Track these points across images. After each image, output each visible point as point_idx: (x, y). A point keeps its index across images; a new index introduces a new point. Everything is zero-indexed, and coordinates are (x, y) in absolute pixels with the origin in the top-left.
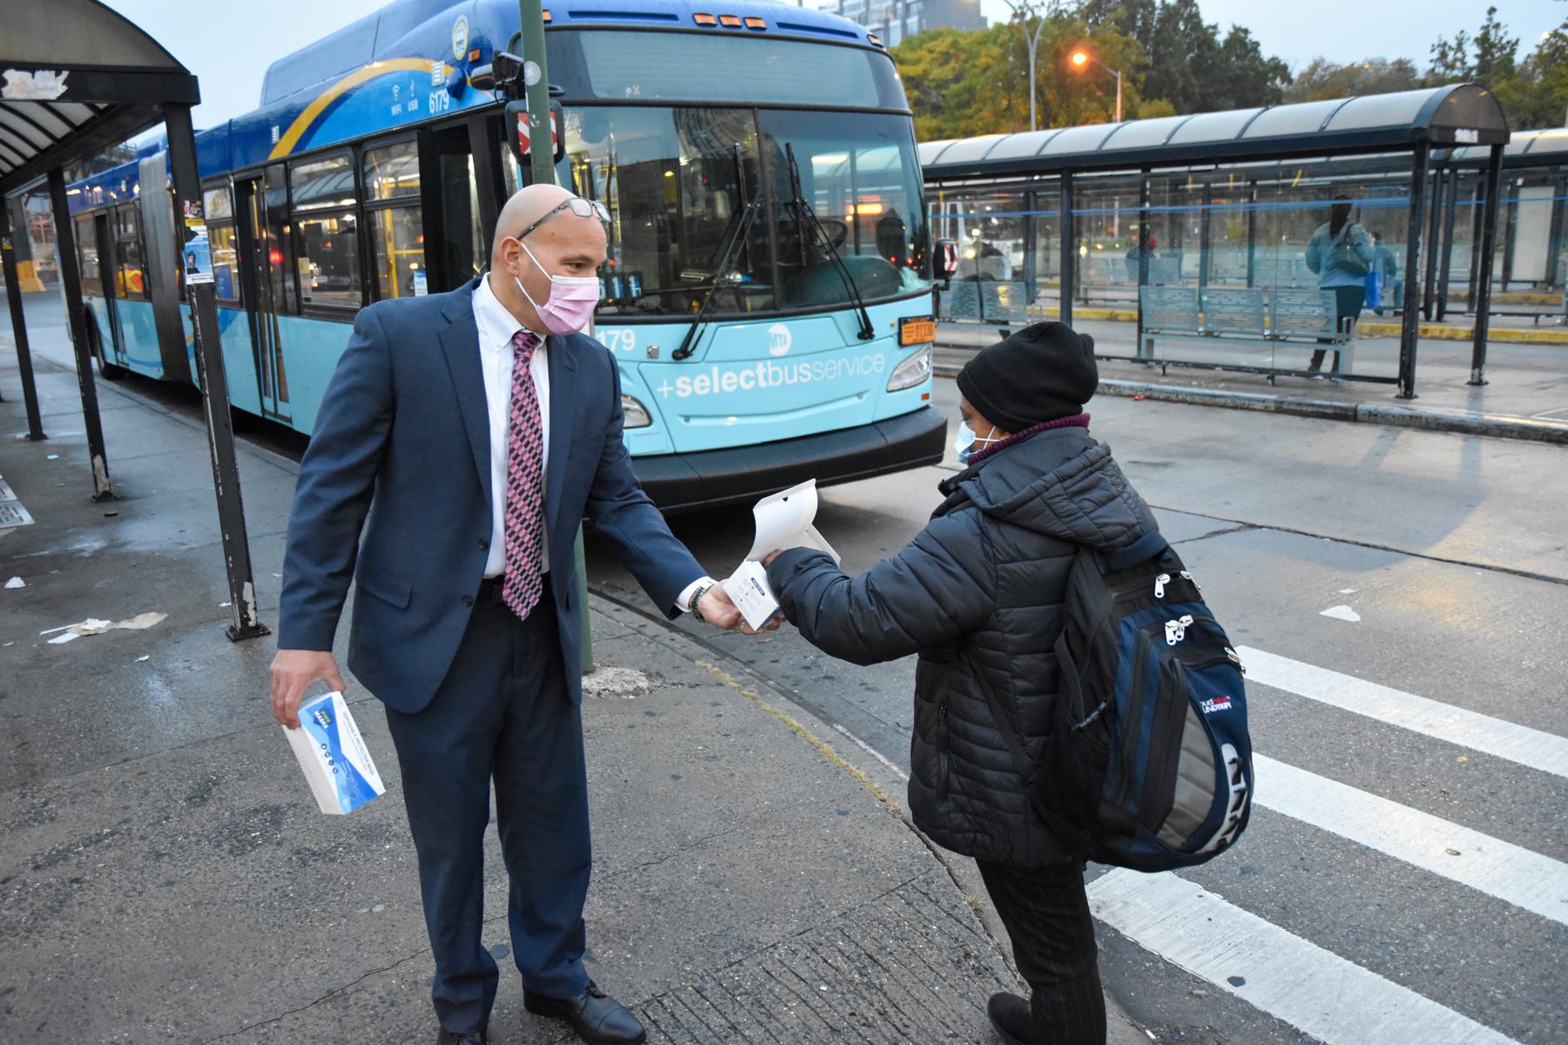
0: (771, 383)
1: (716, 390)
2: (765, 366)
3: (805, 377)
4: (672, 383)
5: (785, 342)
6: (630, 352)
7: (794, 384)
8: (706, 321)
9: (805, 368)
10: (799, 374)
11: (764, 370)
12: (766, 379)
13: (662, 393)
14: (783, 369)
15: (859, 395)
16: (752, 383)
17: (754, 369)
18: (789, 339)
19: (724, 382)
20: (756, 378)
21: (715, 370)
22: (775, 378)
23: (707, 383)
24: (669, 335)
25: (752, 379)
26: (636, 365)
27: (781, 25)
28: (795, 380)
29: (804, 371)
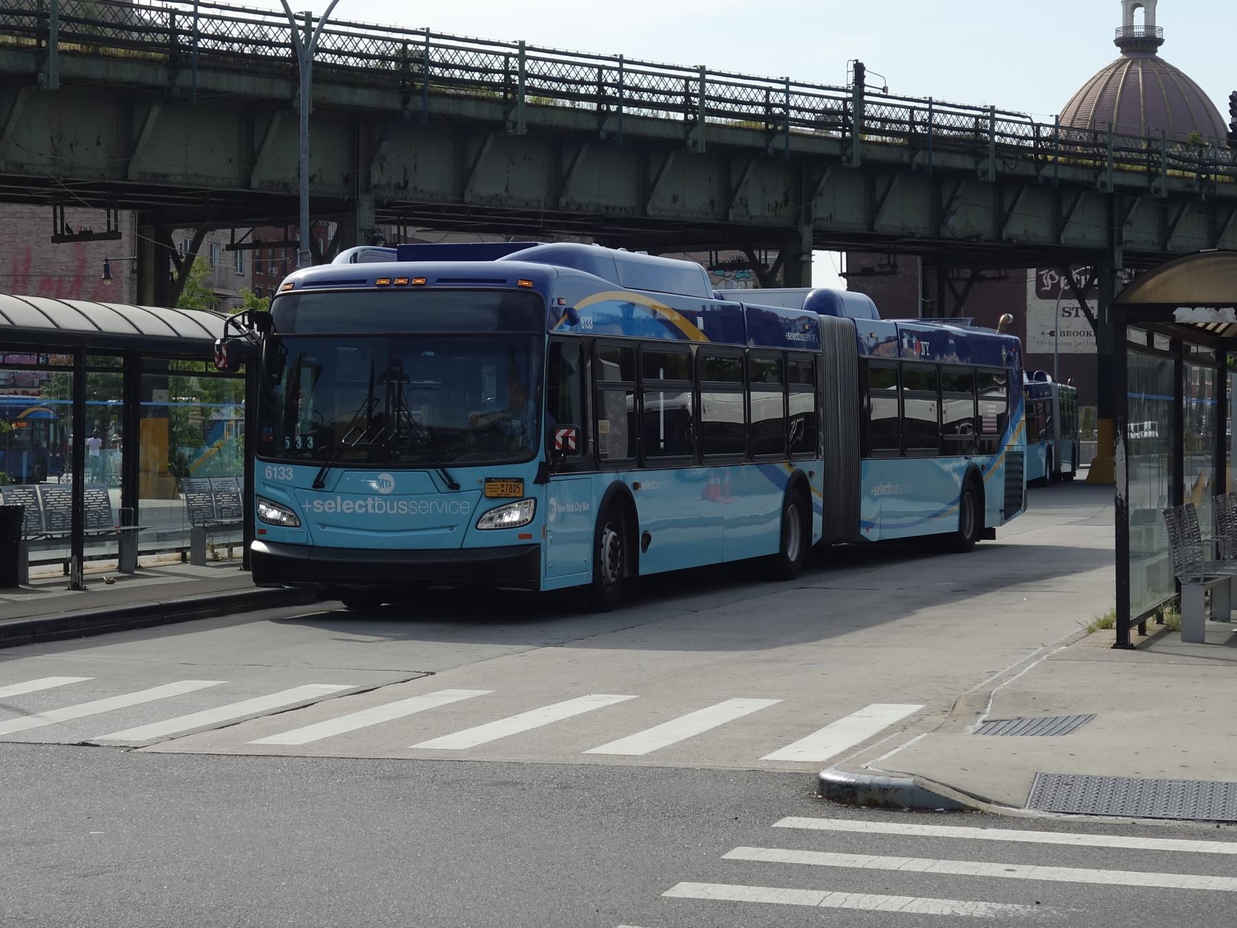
0: (377, 511)
1: (339, 511)
2: (373, 500)
3: (403, 510)
4: (311, 503)
5: (390, 486)
6: (290, 480)
7: (394, 513)
8: (330, 466)
9: (403, 504)
10: (398, 508)
11: (373, 502)
12: (373, 508)
13: (305, 508)
14: (386, 504)
15: (452, 527)
16: (364, 509)
17: (365, 500)
18: (393, 484)
19: (345, 506)
20: (366, 506)
21: (339, 498)
22: (380, 507)
23: (334, 505)
24: (312, 472)
25: (364, 506)
26: (292, 488)
27: (440, 280)
28: (395, 511)
29: (402, 507)
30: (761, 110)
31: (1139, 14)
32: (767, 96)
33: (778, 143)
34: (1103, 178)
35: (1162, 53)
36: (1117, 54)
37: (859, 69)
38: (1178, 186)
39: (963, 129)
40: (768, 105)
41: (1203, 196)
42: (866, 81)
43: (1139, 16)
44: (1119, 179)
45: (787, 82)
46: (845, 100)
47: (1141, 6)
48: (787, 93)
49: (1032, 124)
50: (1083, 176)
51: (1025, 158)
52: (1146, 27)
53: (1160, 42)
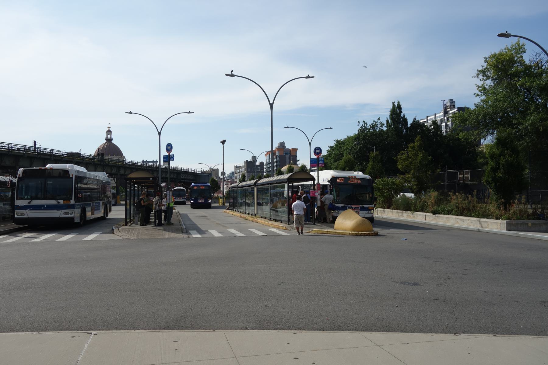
30: (7, 148)
31: (109, 135)
32: (8, 146)
33: (10, 153)
34: (74, 160)
35: (112, 142)
36: (105, 141)
37: (35, 142)
38: (88, 162)
39: (48, 152)
40: (8, 147)
41: (93, 163)
42: (36, 144)
43: (109, 135)
44: (77, 160)
45: (12, 144)
46: (24, 147)
47: (109, 134)
48: (12, 145)
49: (61, 152)
50: (71, 160)
51: (59, 157)
52: (110, 138)
53: (112, 140)
